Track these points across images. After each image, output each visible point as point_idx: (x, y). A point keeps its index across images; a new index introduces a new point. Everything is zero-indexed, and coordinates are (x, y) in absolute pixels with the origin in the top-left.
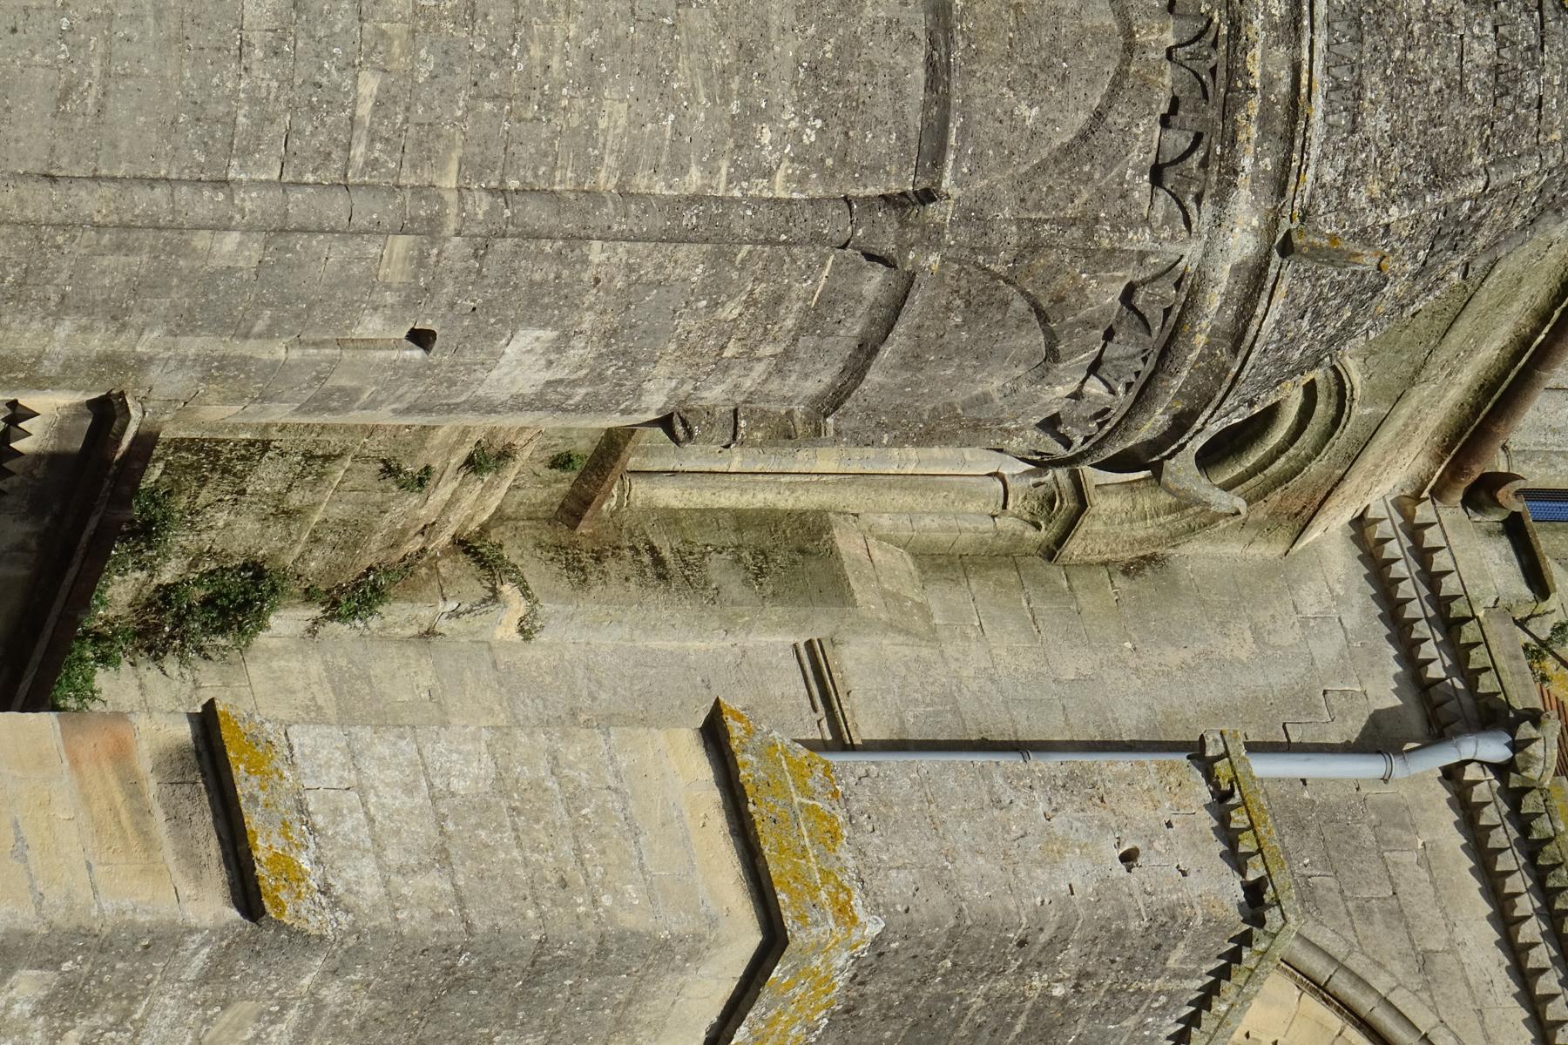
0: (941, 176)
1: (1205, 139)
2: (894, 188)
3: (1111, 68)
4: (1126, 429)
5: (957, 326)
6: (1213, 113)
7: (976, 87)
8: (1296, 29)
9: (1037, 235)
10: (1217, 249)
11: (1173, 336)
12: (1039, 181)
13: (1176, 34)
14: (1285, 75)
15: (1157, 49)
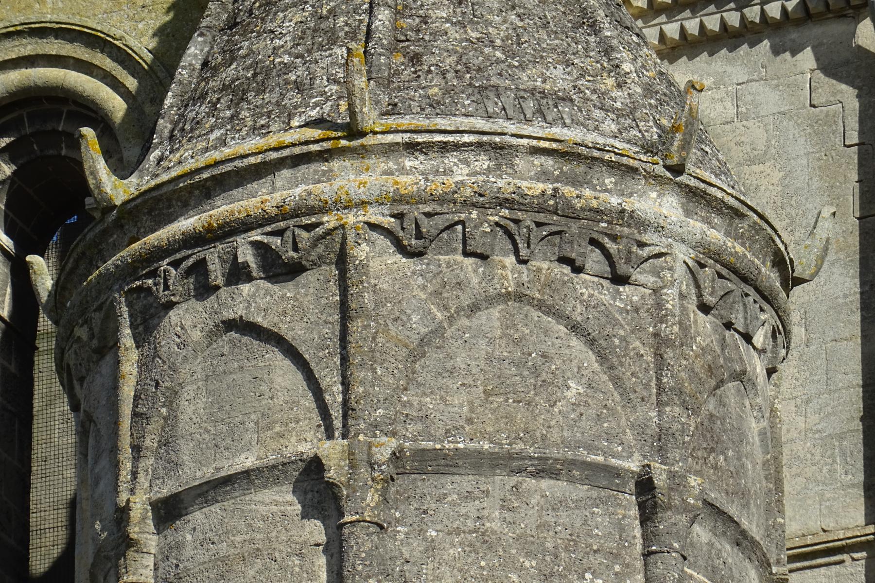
0: (627, 471)
1: (595, 236)
2: (634, 512)
3: (535, 314)
4: (784, 312)
5: (725, 460)
6: (574, 227)
7: (555, 436)
8: (502, 148)
9: (672, 389)
10: (680, 231)
11: (735, 271)
12: (628, 384)
13: (506, 255)
14: (538, 160)
15: (519, 272)
